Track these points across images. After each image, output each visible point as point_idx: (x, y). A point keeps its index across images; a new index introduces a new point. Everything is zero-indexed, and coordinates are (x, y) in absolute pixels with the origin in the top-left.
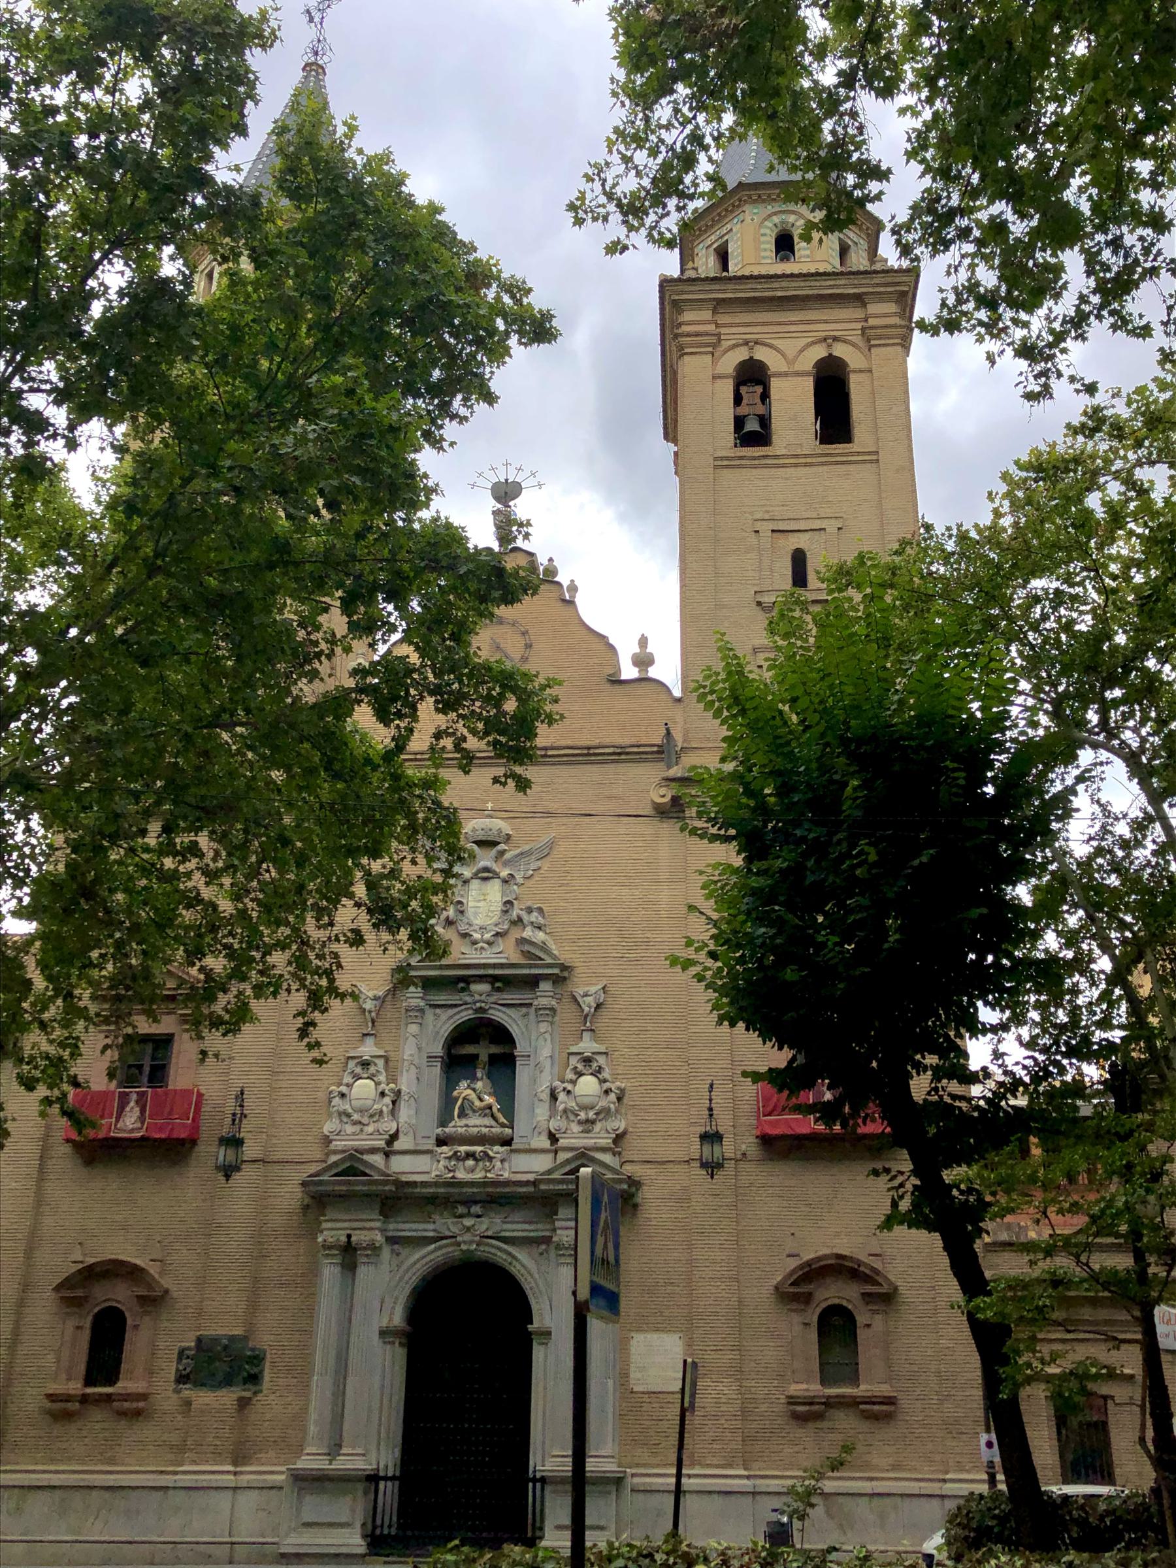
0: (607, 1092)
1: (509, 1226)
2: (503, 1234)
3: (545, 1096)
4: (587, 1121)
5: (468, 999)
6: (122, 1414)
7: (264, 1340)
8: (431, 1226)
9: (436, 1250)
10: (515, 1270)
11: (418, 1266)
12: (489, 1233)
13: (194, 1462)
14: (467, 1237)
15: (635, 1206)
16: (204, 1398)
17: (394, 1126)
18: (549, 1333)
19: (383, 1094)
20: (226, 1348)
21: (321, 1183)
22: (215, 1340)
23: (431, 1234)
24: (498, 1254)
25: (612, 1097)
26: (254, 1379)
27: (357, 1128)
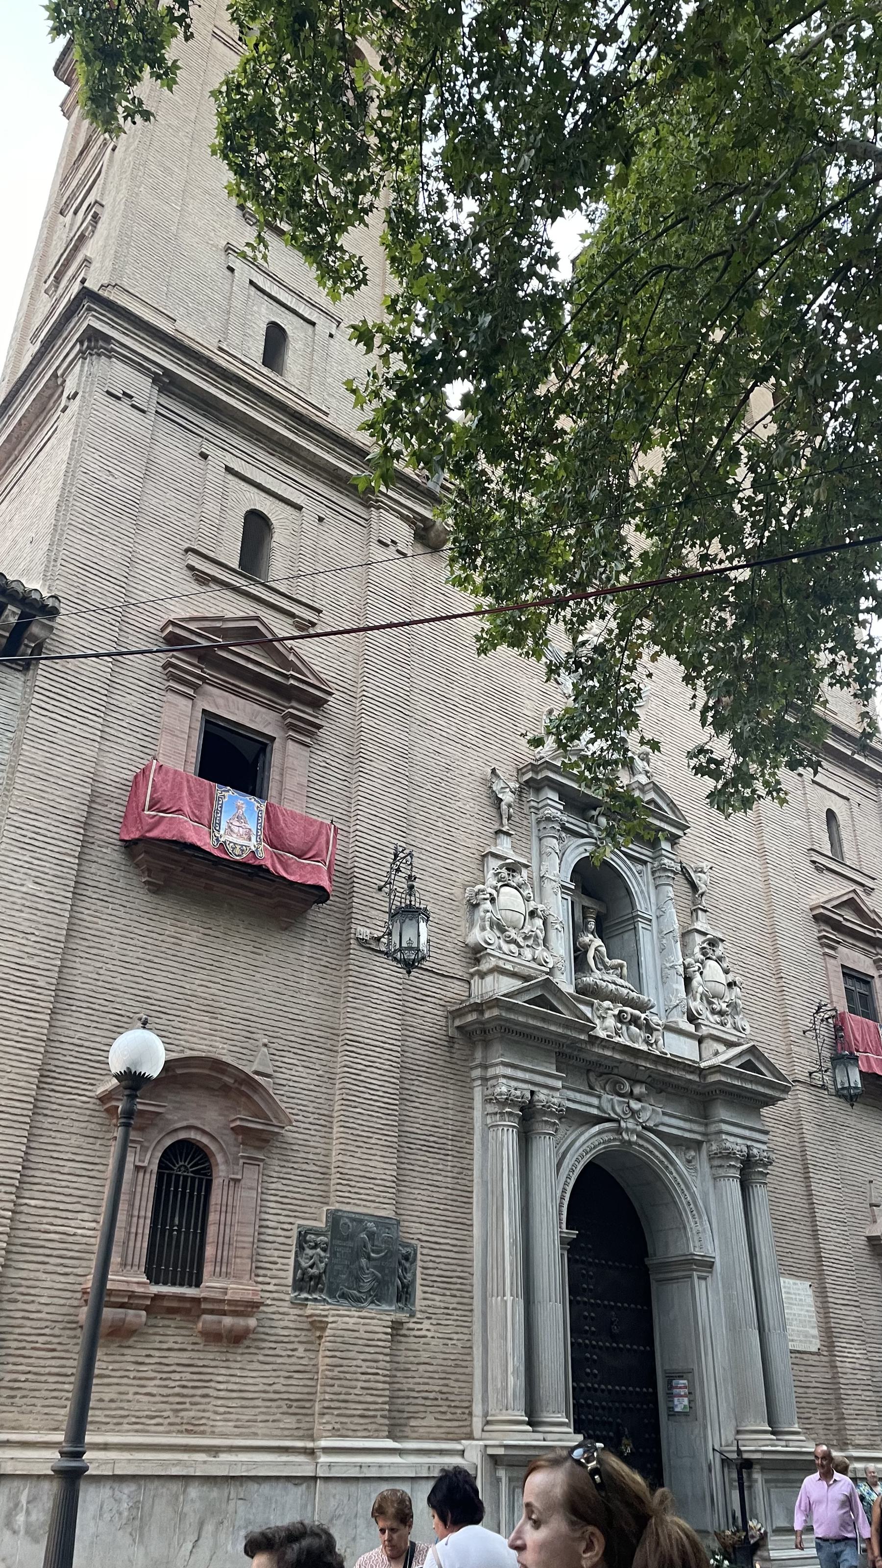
1: (667, 1120)
2: (662, 1128)
6: (213, 1337)
7: (414, 1231)
8: (595, 1101)
9: (600, 1133)
10: (671, 1176)
12: (651, 1124)
13: (336, 1433)
14: (631, 1124)
16: (344, 1318)
18: (711, 1265)
20: (371, 1235)
21: (512, 1008)
22: (358, 1220)
23: (595, 1111)
24: (656, 1151)
26: (405, 1295)
27: (513, 947)
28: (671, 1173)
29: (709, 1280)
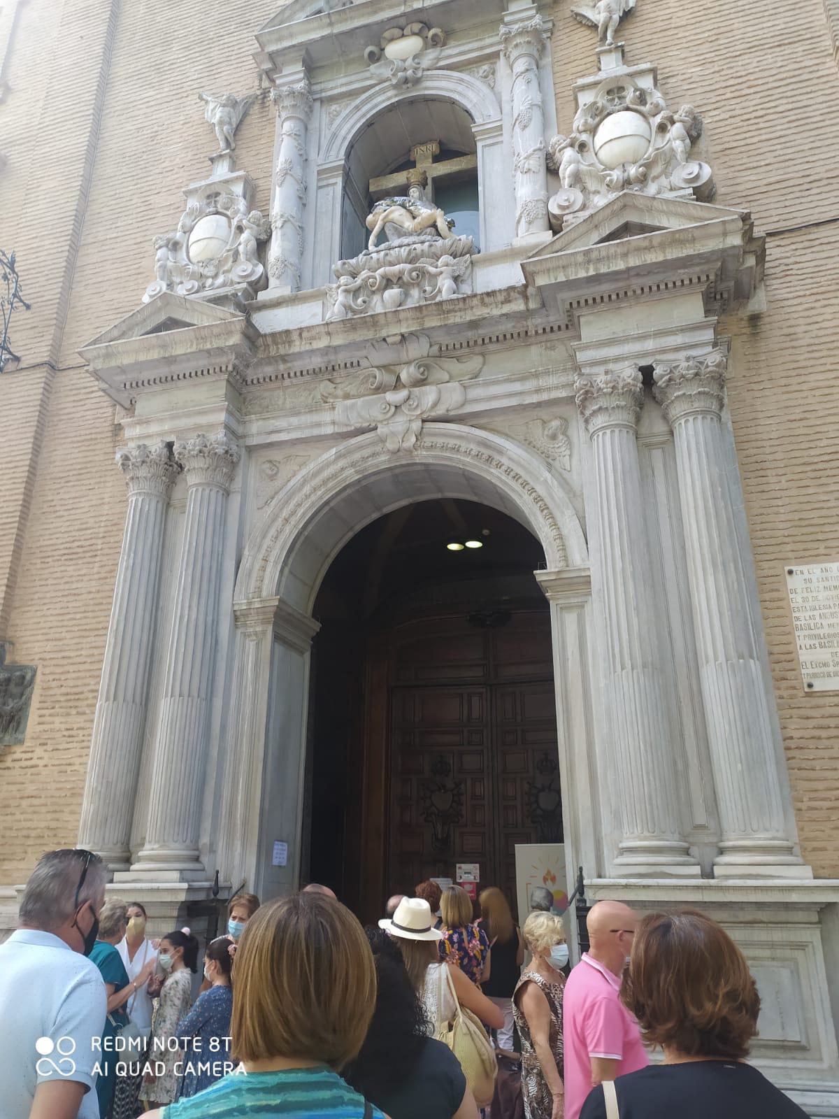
0: (662, 128)
3: (536, 163)
4: (627, 182)
5: (387, 73)
11: (307, 489)
15: (755, 319)
17: (260, 269)
18: (587, 581)
19: (240, 229)
25: (676, 130)
28: (499, 465)
29: (587, 608)
